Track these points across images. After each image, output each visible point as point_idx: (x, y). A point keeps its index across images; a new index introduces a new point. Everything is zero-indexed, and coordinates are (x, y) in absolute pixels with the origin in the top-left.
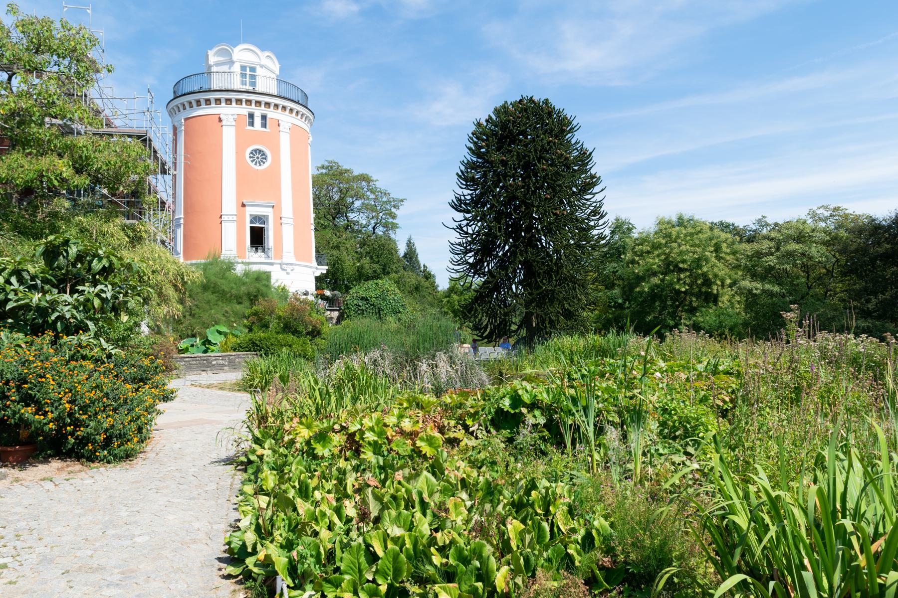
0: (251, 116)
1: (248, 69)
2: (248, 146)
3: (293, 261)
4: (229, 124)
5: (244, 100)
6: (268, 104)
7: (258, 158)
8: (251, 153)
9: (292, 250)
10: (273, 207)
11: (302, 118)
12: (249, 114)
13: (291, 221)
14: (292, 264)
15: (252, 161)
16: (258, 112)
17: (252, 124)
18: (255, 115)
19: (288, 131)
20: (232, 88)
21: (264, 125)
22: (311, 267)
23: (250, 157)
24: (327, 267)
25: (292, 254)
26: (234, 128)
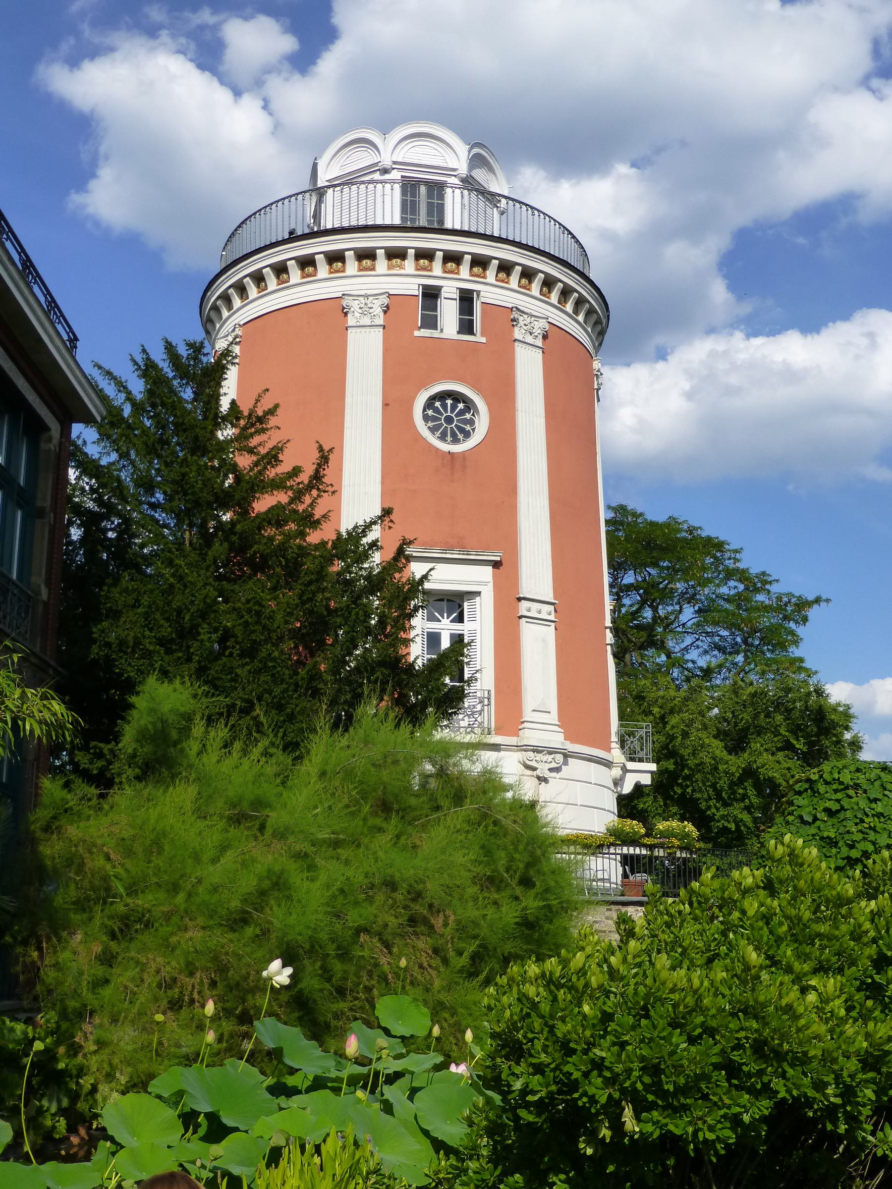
0: (431, 295)
1: (423, 189)
2: (424, 385)
3: (557, 739)
4: (366, 321)
5: (411, 252)
6: (480, 262)
7: (449, 420)
8: (429, 404)
9: (553, 705)
10: (496, 565)
11: (576, 311)
12: (425, 295)
13: (547, 612)
14: (551, 751)
15: (433, 430)
16: (450, 289)
17: (430, 322)
18: (444, 294)
19: (539, 343)
20: (379, 222)
21: (467, 327)
22: (608, 764)
23: (426, 418)
24: (653, 767)
25: (554, 717)
26: (379, 334)
